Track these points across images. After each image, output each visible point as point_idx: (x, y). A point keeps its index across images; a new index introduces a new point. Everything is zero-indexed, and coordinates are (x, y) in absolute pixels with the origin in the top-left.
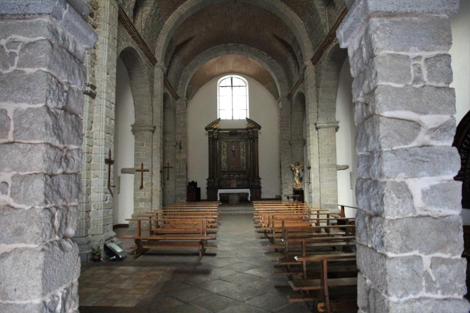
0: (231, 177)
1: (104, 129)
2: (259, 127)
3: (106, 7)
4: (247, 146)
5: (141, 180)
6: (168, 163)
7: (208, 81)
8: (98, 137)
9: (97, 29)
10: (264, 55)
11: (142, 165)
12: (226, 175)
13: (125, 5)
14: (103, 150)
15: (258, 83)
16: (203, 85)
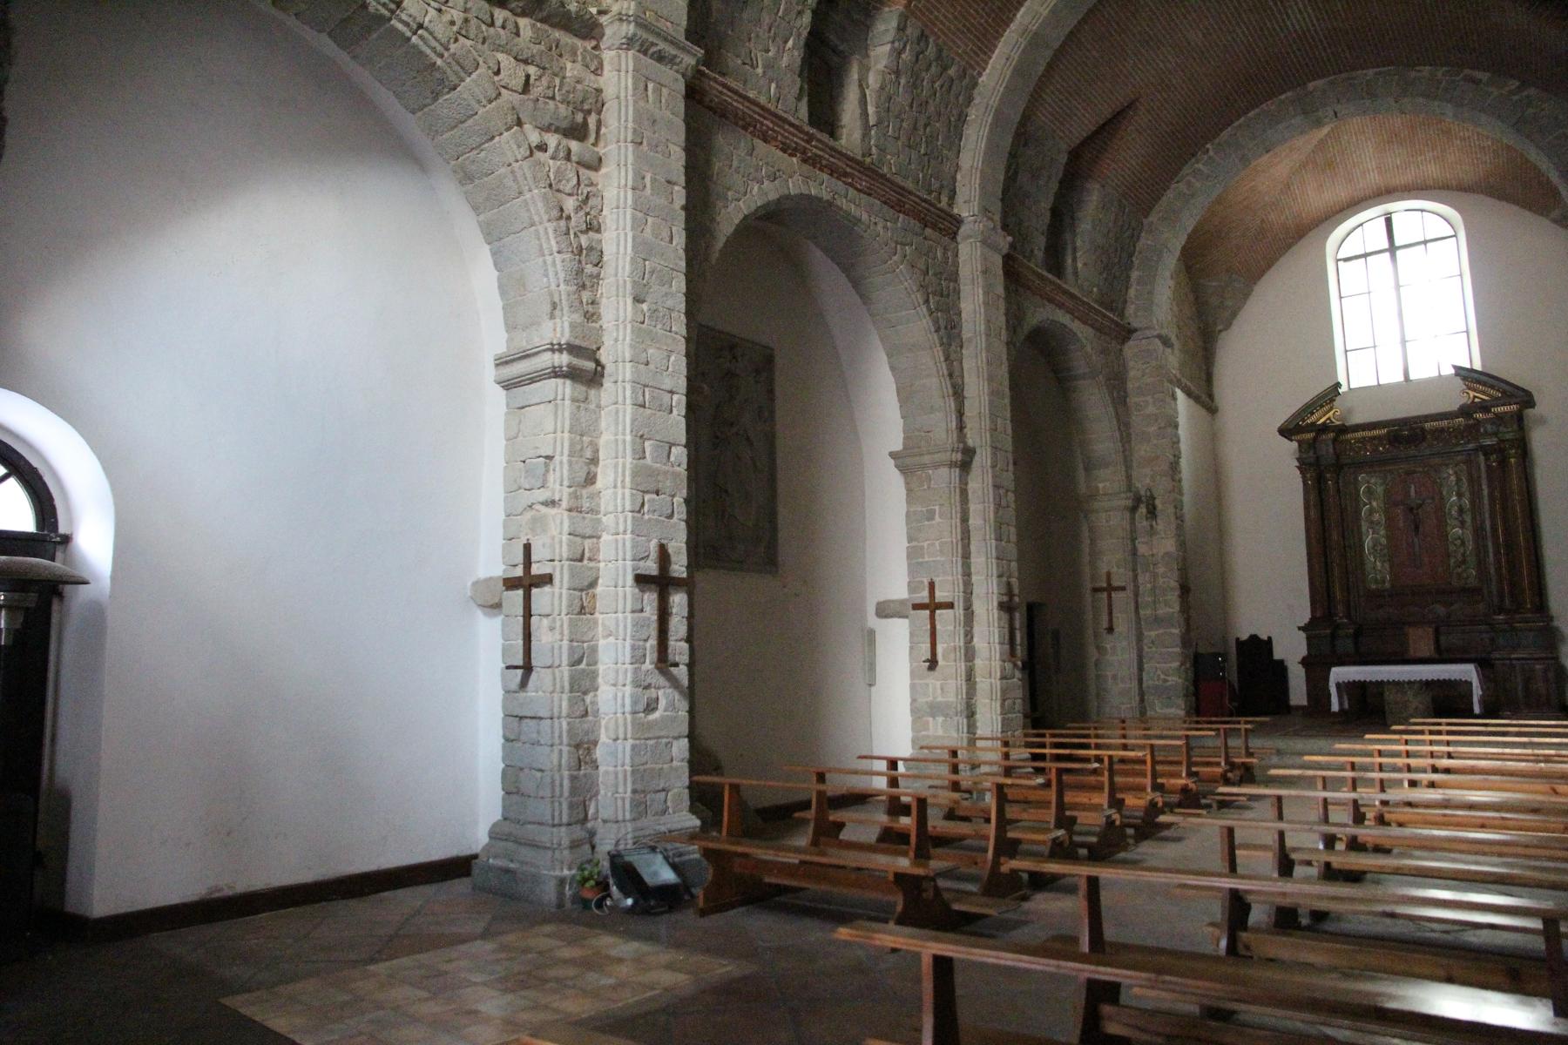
1: (628, 479)
3: (623, 95)
4: (1474, 482)
5: (928, 640)
6: (1109, 575)
8: (611, 508)
9: (603, 171)
10: (1476, 82)
11: (932, 586)
13: (754, 67)
14: (628, 544)
15: (1515, 208)
16: (1269, 267)
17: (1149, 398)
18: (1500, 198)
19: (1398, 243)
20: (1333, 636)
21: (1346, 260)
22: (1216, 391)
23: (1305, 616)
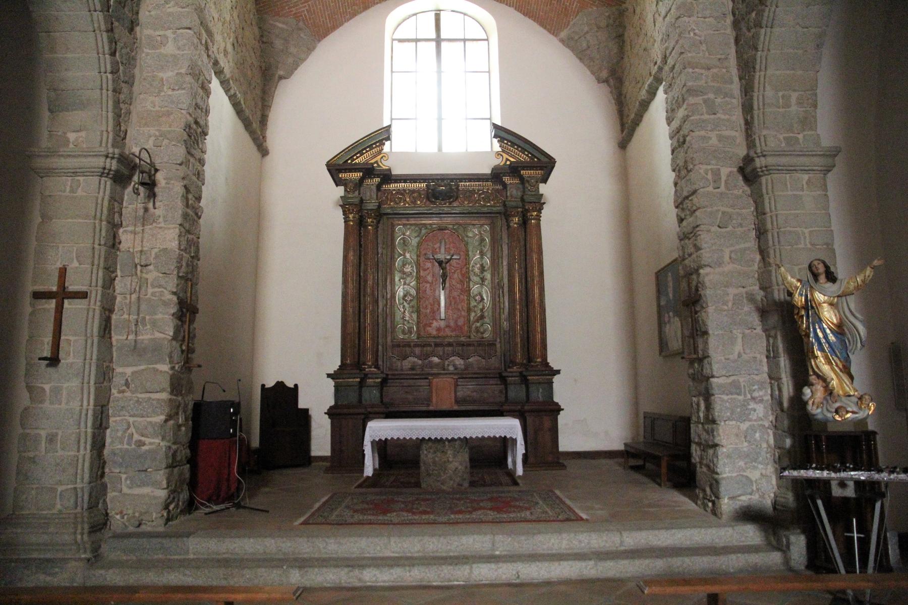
0: (432, 365)
2: (544, 165)
4: (495, 242)
6: (63, 272)
7: (354, 15)
12: (412, 359)
16: (334, 28)
17: (169, 33)
18: (525, 14)
19: (443, 36)
20: (362, 384)
21: (401, 41)
22: (269, 133)
23: (335, 363)
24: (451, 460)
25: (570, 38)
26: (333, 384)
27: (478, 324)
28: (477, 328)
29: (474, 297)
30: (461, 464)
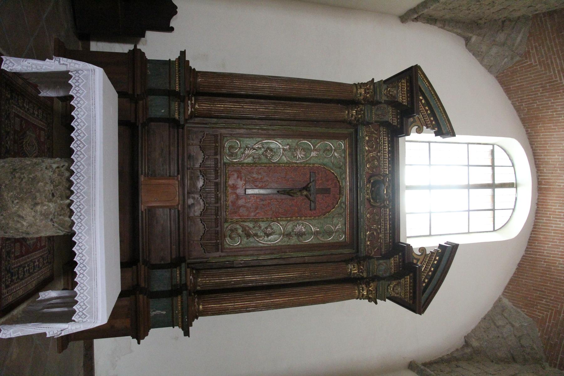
0: (194, 179)
7: (518, 110)
18: (520, 265)
19: (497, 190)
20: (171, 94)
21: (493, 152)
22: (419, 25)
23: (197, 65)
24: (39, 208)
25: (504, 309)
26: (173, 59)
27: (240, 231)
28: (236, 229)
29: (270, 226)
30: (31, 225)
